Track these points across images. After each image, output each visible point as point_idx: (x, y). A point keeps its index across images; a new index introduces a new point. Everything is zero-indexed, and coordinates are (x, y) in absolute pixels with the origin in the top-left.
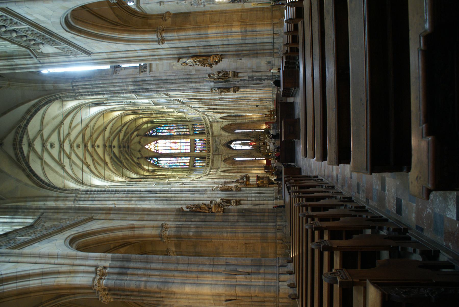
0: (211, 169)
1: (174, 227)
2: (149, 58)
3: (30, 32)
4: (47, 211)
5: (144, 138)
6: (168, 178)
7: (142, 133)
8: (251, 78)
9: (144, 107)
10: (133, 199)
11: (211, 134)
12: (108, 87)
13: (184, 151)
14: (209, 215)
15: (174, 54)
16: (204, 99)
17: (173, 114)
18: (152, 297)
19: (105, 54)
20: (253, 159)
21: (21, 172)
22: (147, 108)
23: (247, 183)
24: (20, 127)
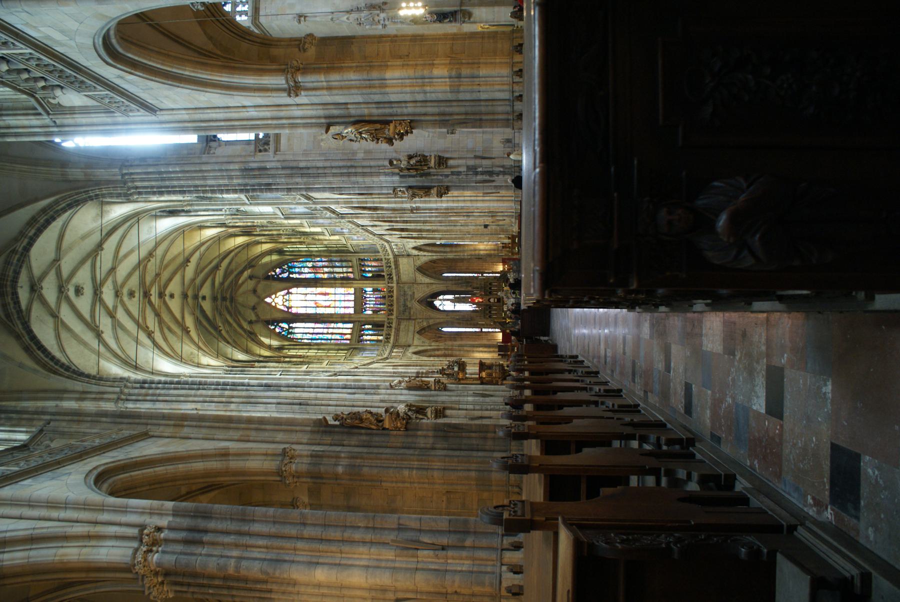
0: (394, 347)
1: (307, 456)
2: (270, 122)
3: (33, 63)
4: (58, 417)
5: (263, 283)
6: (309, 363)
7: (260, 272)
8: (473, 170)
9: (265, 221)
10: (233, 400)
12: (193, 178)
13: (342, 311)
14: (377, 434)
15: (319, 117)
16: (382, 209)
17: (321, 237)
18: (251, 590)
19: (184, 112)
20: (477, 330)
22: (271, 223)
23: (461, 376)
24: (14, 251)
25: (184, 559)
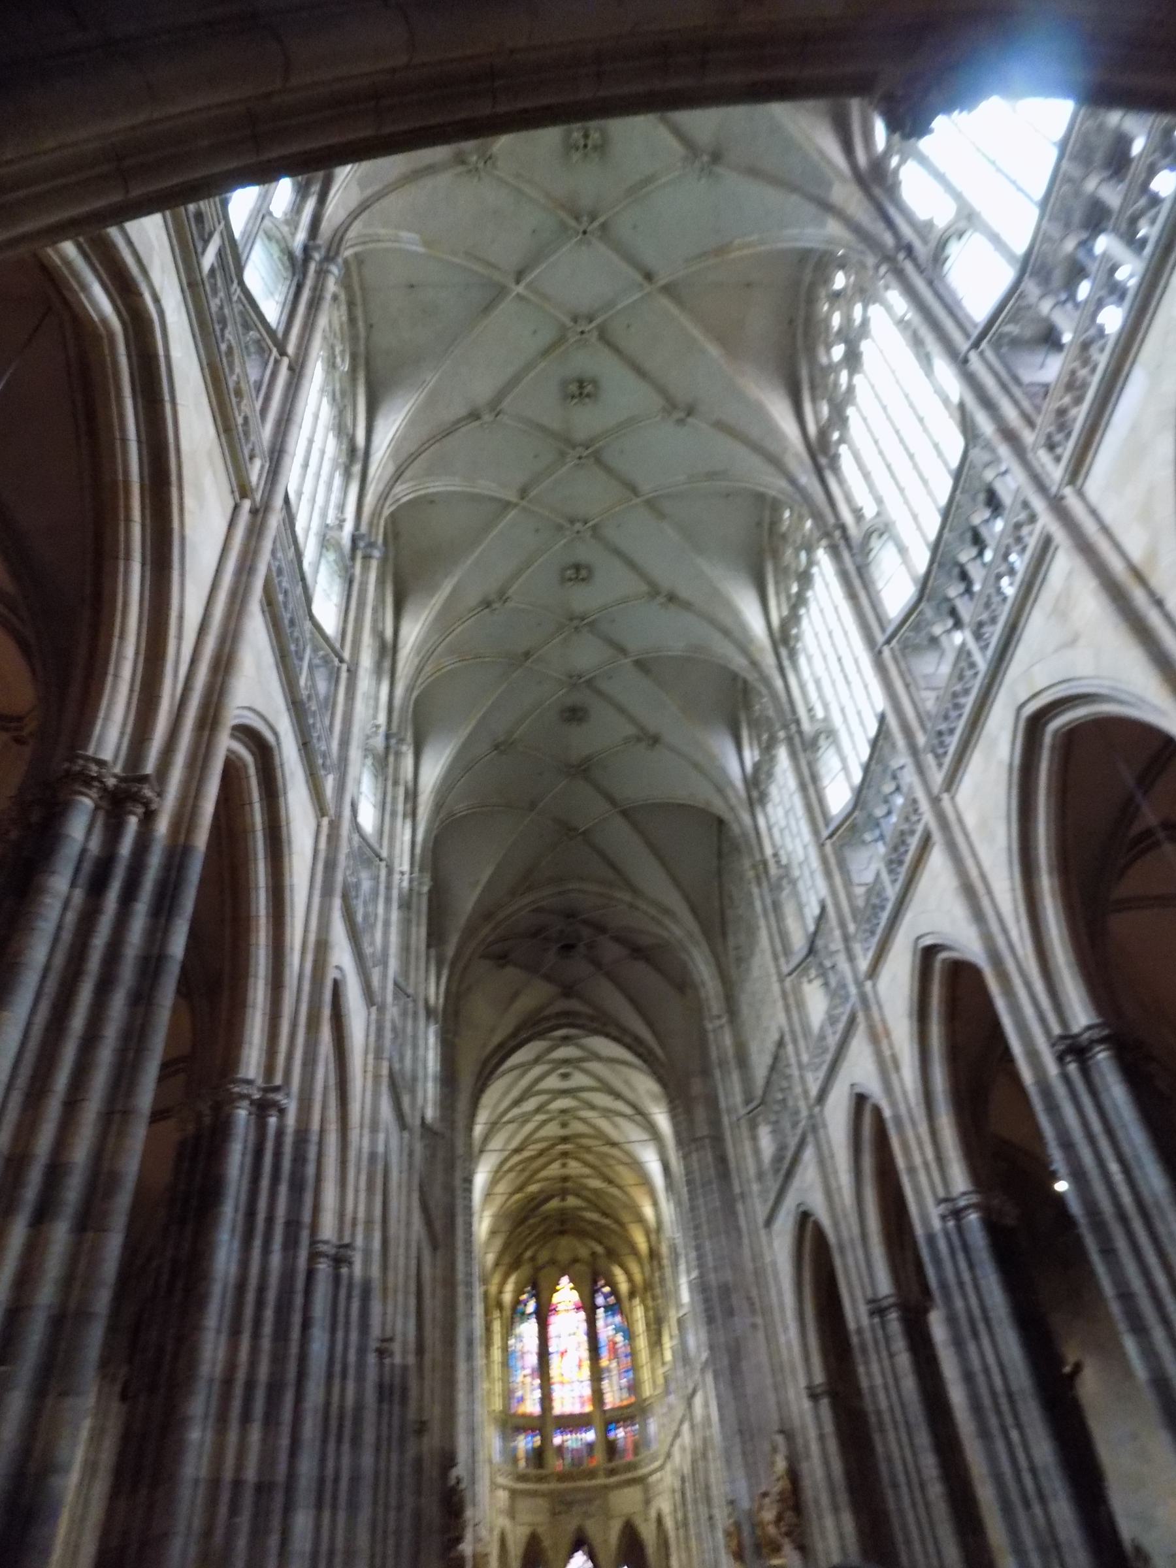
11: (613, 1480)
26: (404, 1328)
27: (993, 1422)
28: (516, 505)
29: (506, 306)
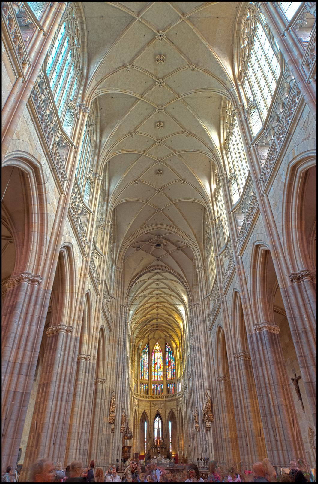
7: (168, 340)
11: (167, 399)
13: (153, 375)
21: (140, 270)
23: (126, 438)
24: (169, 269)
25: (82, 368)
26: (94, 353)
27: (264, 391)
28: (139, 99)
29: (135, 24)
